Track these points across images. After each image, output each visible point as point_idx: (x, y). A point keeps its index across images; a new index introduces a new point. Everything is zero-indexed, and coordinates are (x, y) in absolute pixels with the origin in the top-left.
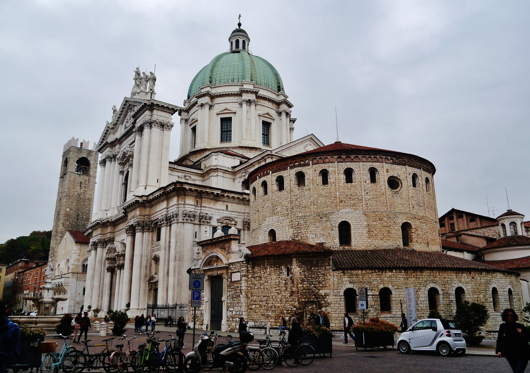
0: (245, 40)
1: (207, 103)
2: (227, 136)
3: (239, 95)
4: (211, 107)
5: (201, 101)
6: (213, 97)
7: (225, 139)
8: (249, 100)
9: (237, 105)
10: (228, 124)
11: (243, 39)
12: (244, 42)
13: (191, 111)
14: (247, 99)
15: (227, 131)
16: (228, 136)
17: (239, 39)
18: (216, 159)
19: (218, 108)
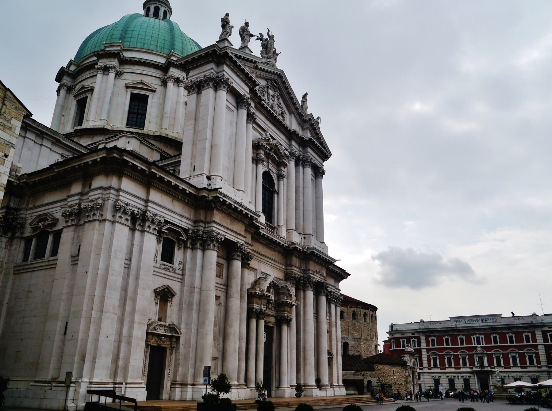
0: (168, 11)
1: (114, 67)
2: (137, 120)
3: (164, 68)
4: (118, 74)
5: (102, 63)
6: (124, 62)
7: (134, 123)
8: (178, 78)
9: (158, 82)
10: (141, 104)
11: (164, 9)
12: (165, 12)
13: (80, 78)
14: (176, 77)
15: (138, 114)
16: (139, 120)
17: (160, 6)
18: (129, 143)
19: (128, 79)
